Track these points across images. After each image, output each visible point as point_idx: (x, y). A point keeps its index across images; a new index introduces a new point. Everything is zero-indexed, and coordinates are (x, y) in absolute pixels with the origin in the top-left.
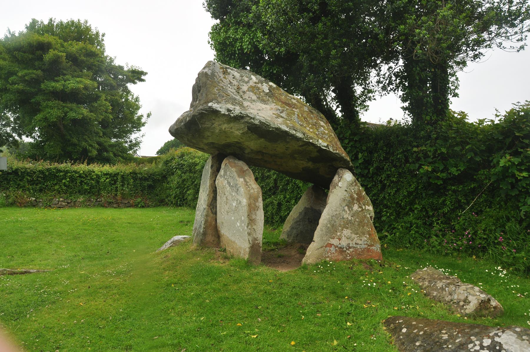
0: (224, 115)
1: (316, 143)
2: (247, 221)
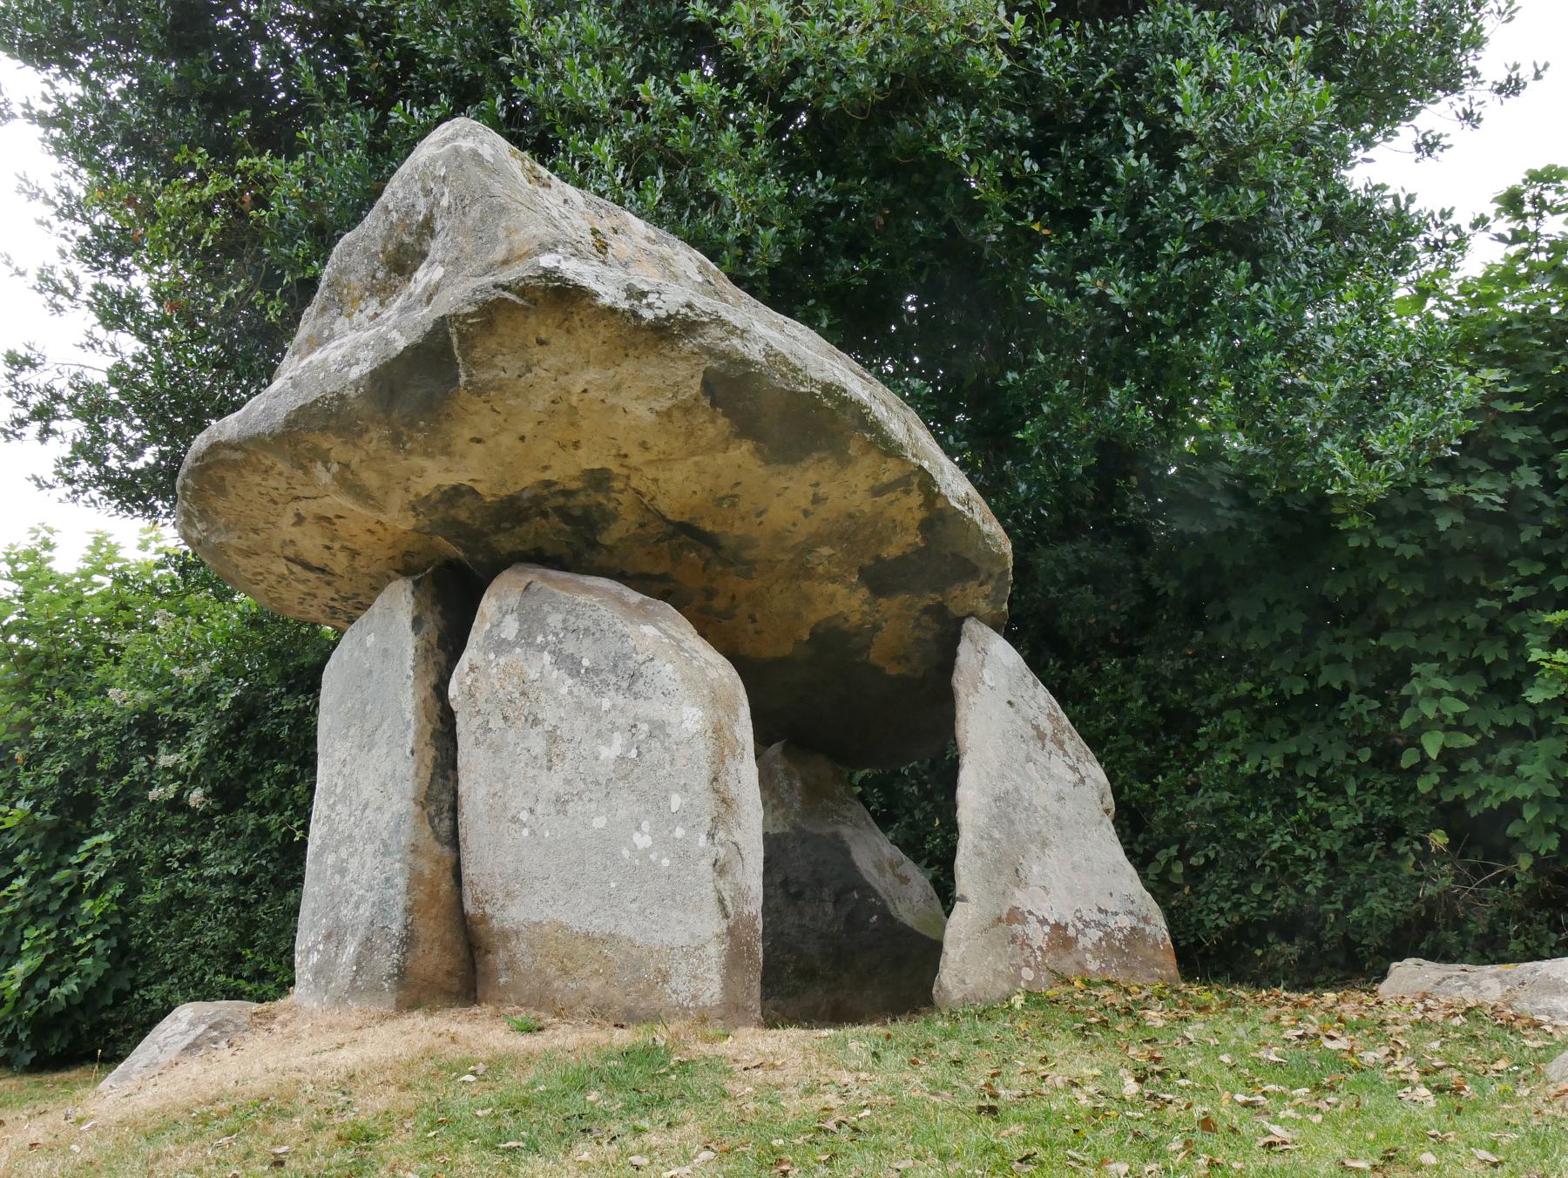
0: (612, 310)
2: (707, 805)
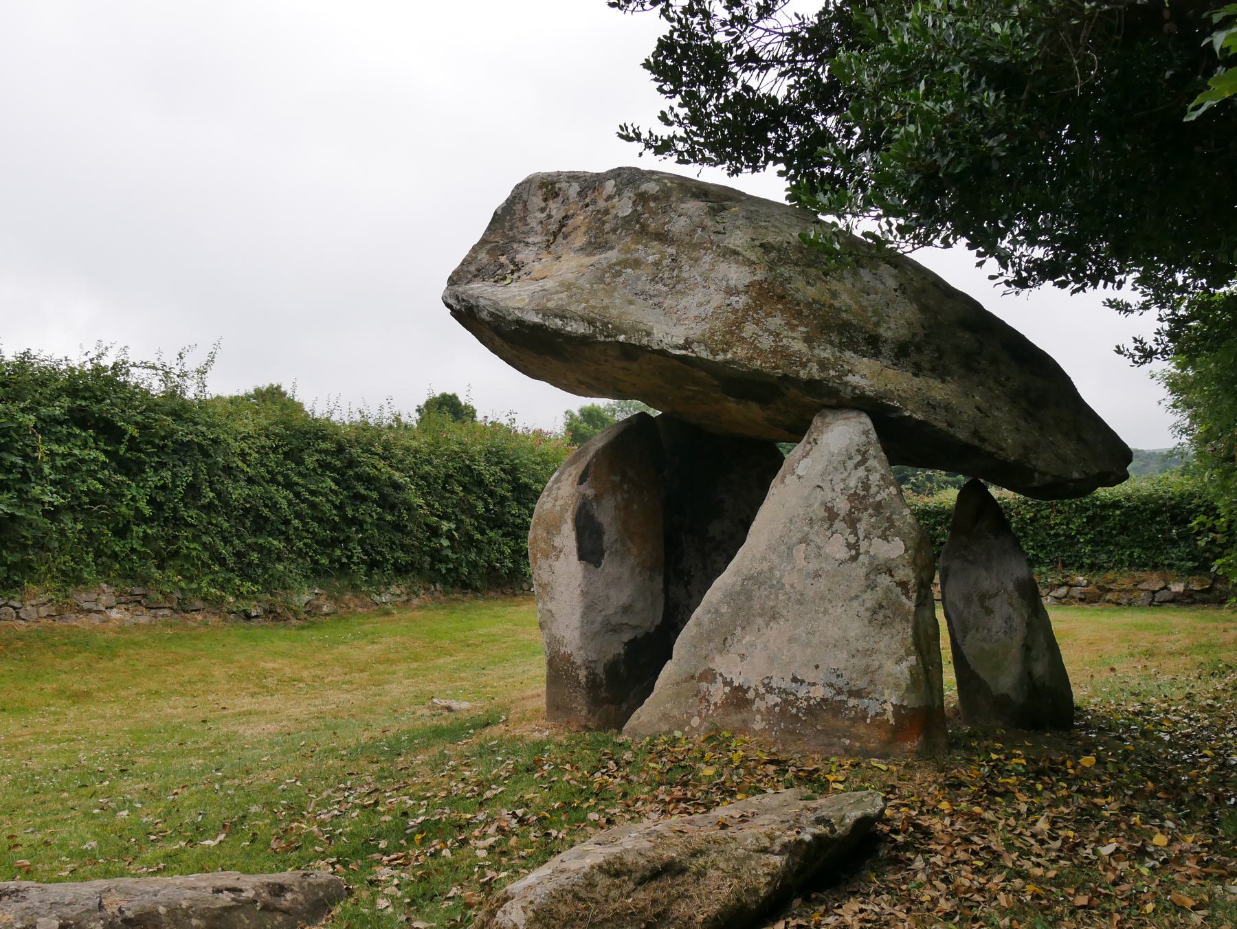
1: (645, 341)
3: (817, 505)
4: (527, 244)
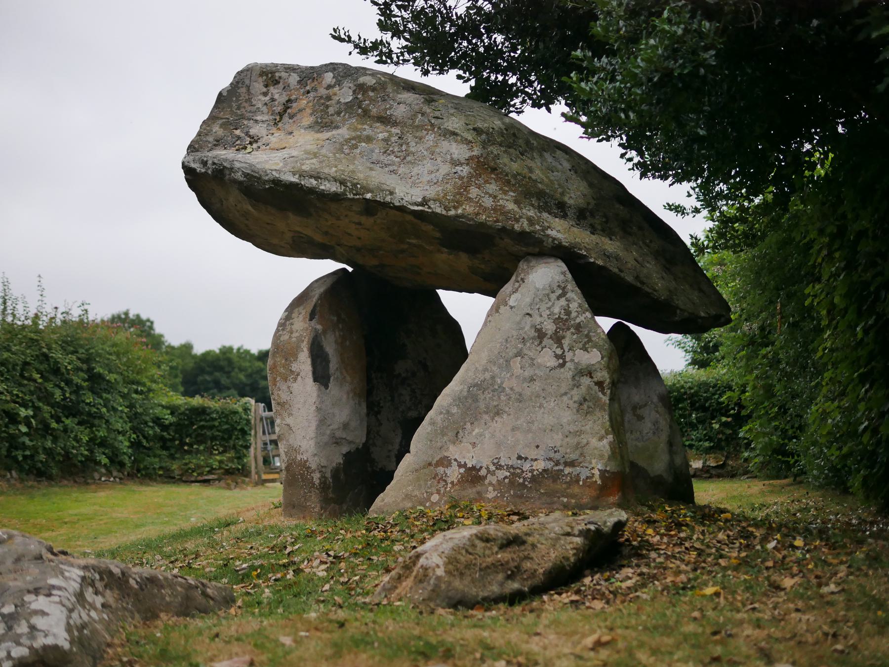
1: (388, 199)
3: (527, 328)
4: (256, 121)
